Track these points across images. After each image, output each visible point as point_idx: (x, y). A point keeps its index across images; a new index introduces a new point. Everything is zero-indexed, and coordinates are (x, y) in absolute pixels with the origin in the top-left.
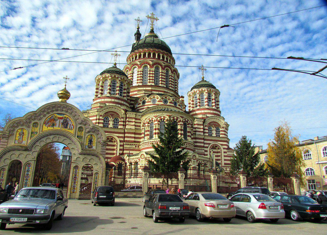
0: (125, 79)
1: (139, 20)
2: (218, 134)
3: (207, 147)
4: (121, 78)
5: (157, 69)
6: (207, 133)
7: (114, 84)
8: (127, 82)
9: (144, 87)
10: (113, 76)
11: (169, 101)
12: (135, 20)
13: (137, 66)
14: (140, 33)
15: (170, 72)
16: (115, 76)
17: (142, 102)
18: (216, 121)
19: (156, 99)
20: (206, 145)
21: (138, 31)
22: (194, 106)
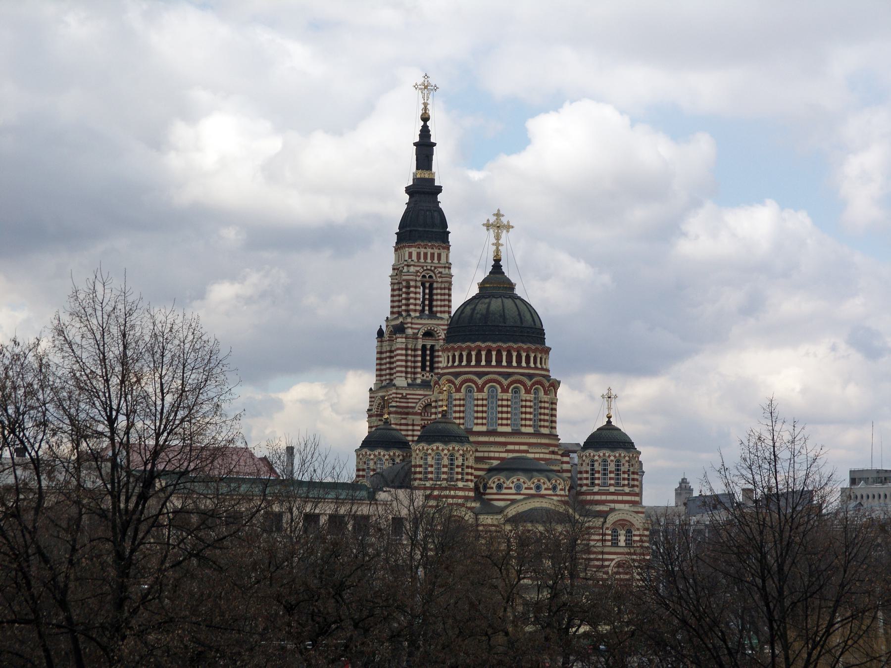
0: (469, 449)
1: (426, 87)
2: (629, 540)
3: (609, 566)
4: (463, 450)
5: (516, 392)
6: (609, 541)
7: (452, 460)
8: (471, 452)
9: (491, 436)
10: (451, 448)
11: (544, 487)
12: (416, 87)
13: (473, 386)
14: (433, 140)
15: (542, 393)
16: (454, 448)
17: (496, 484)
18: (627, 519)
19: (523, 484)
20: (606, 563)
21: (425, 132)
22: (588, 482)
